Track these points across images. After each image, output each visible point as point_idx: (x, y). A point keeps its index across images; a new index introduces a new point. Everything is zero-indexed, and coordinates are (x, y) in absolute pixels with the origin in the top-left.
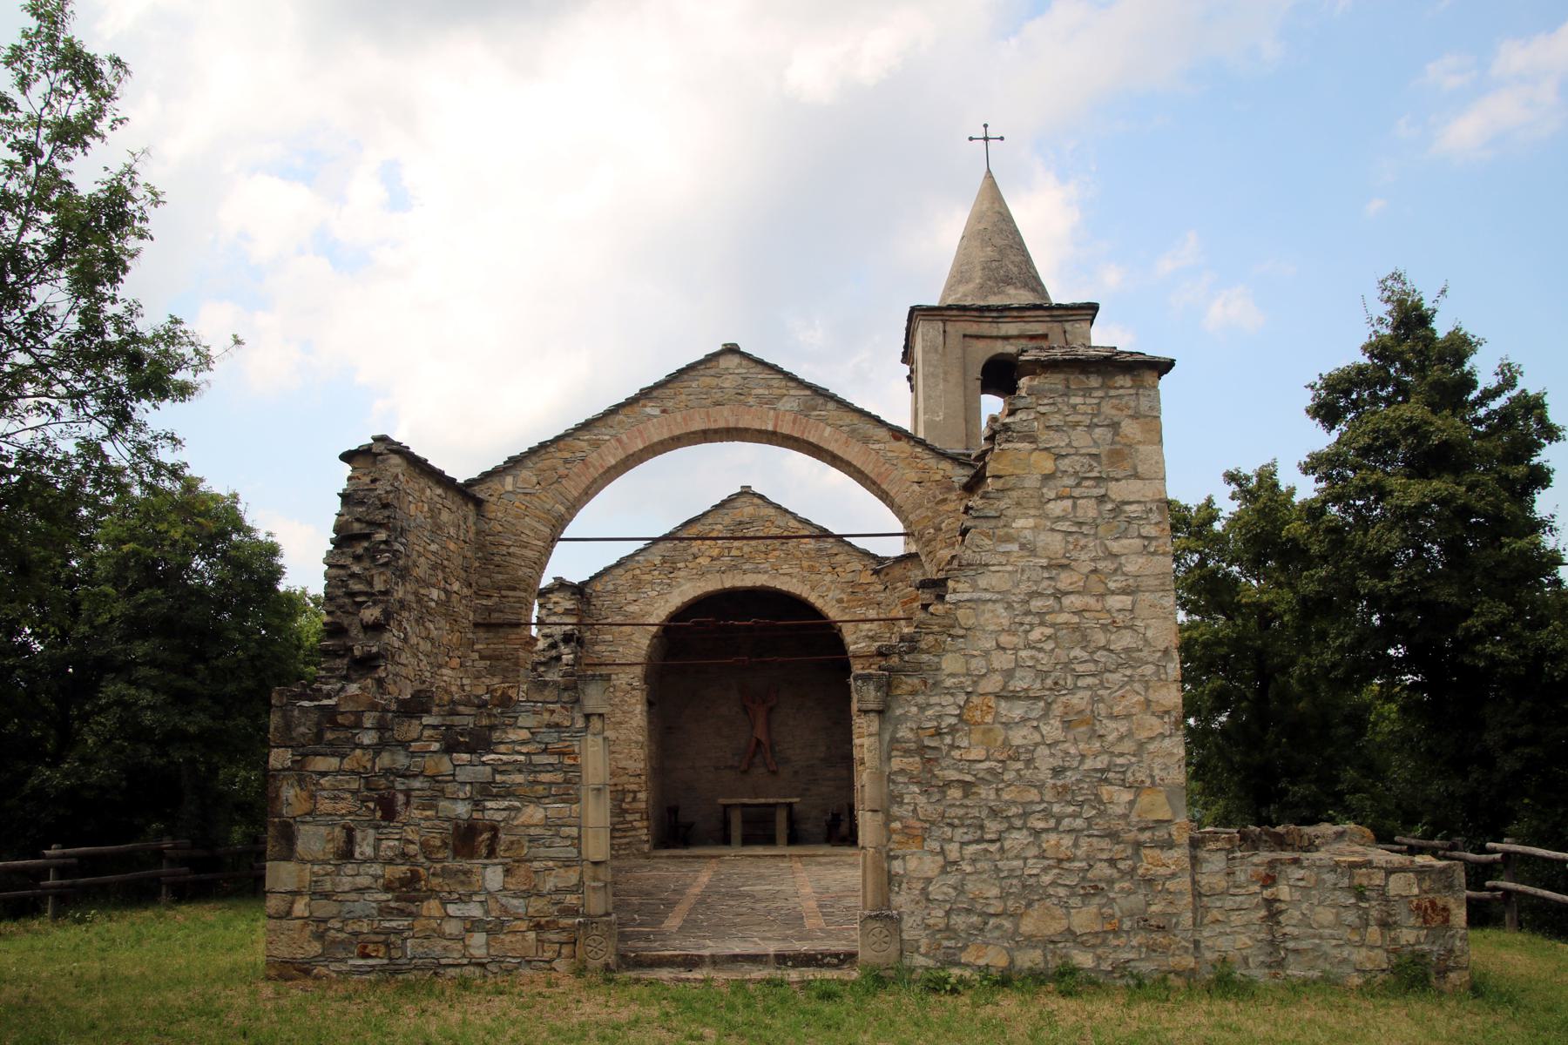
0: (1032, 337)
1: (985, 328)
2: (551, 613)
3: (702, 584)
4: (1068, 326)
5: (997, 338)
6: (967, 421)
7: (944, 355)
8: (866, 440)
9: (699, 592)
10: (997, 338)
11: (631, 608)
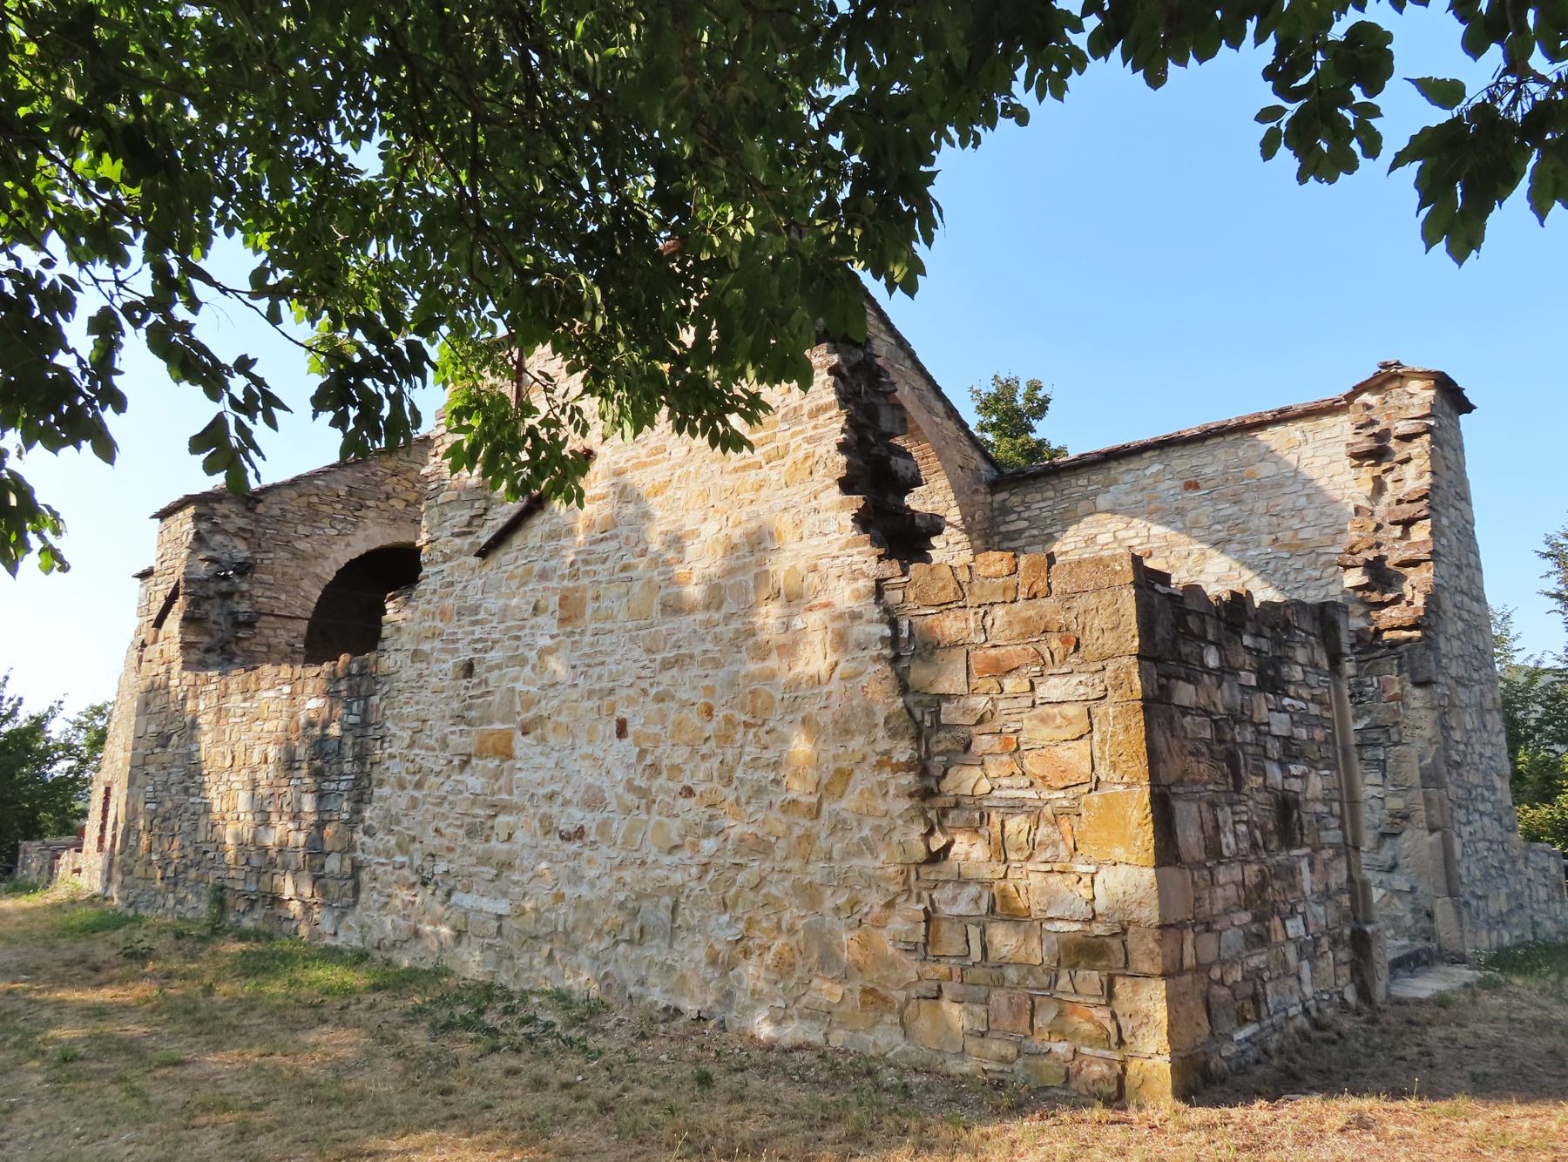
2: (217, 529)
3: (394, 532)
8: (930, 411)
9: (388, 541)
11: (301, 545)
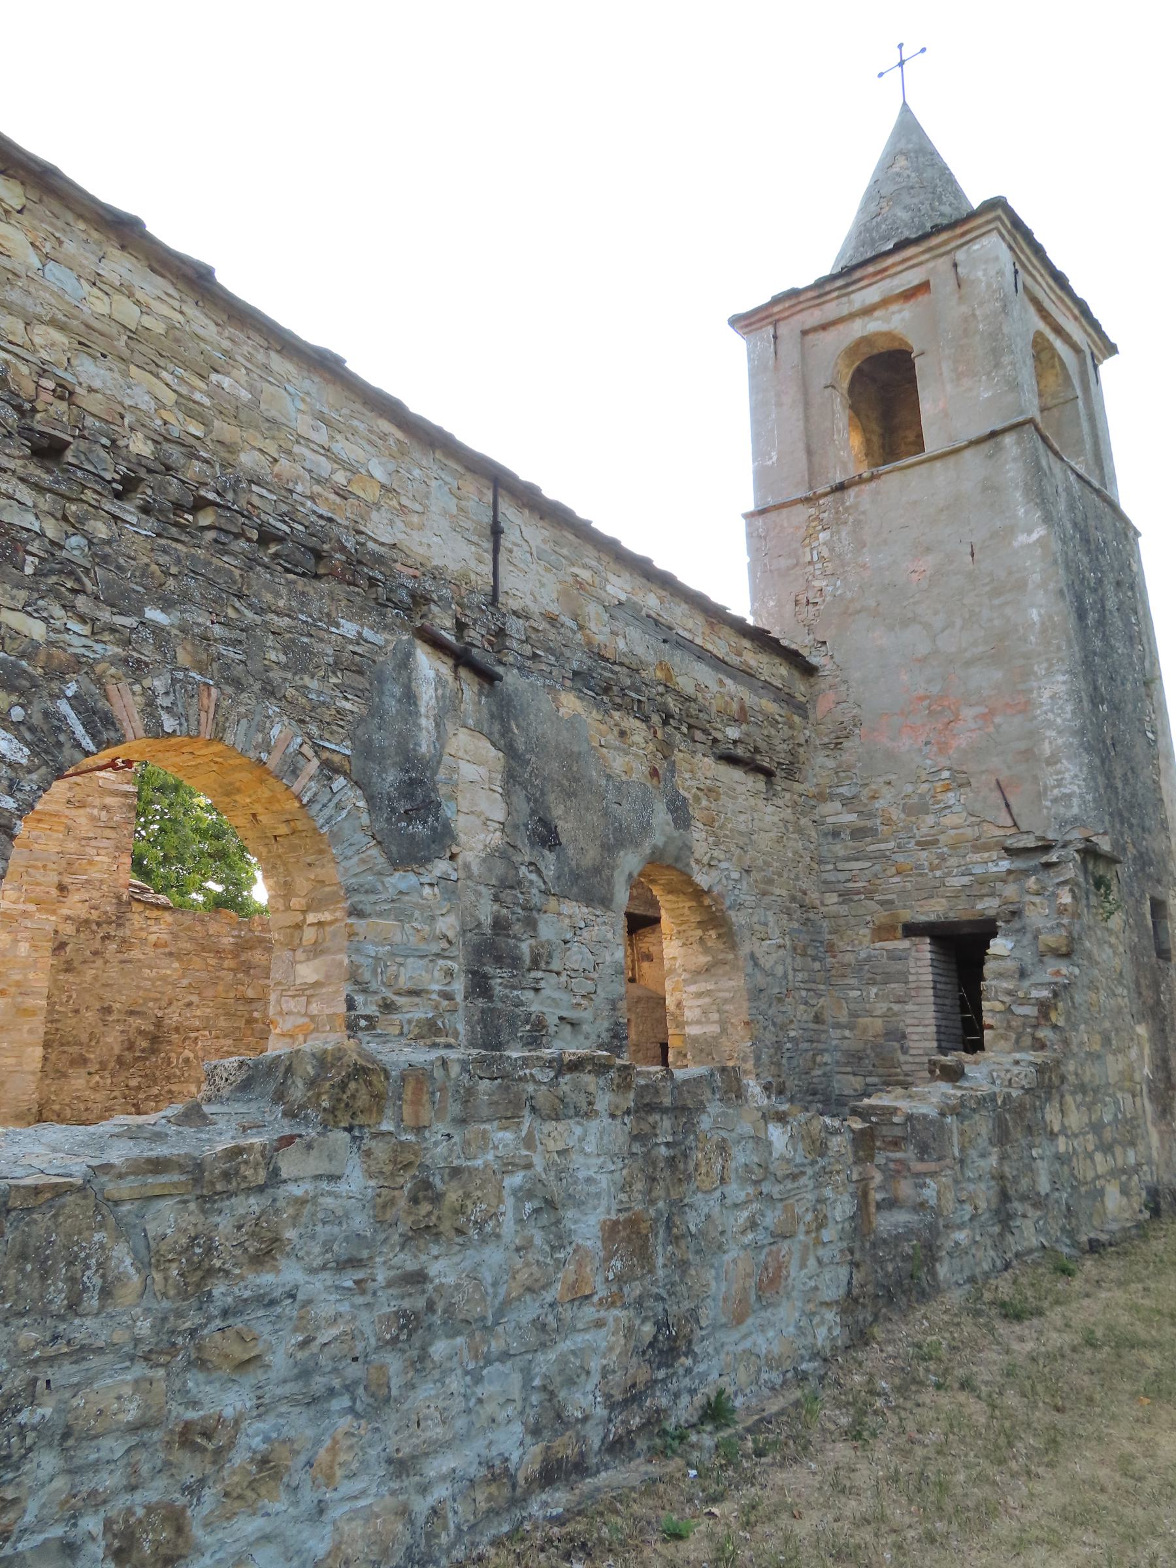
0: (908, 295)
1: (832, 310)
4: (960, 256)
5: (852, 316)
6: (809, 452)
7: (776, 368)
10: (852, 316)
